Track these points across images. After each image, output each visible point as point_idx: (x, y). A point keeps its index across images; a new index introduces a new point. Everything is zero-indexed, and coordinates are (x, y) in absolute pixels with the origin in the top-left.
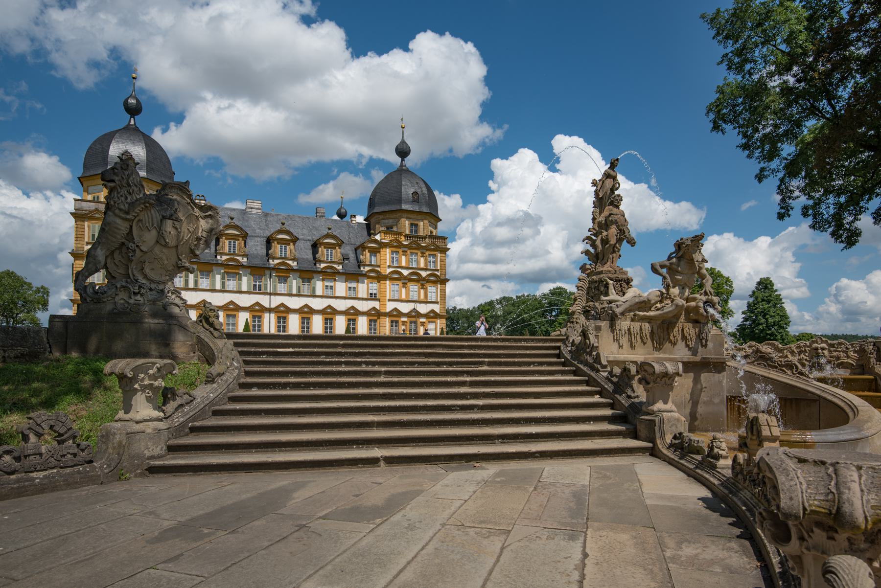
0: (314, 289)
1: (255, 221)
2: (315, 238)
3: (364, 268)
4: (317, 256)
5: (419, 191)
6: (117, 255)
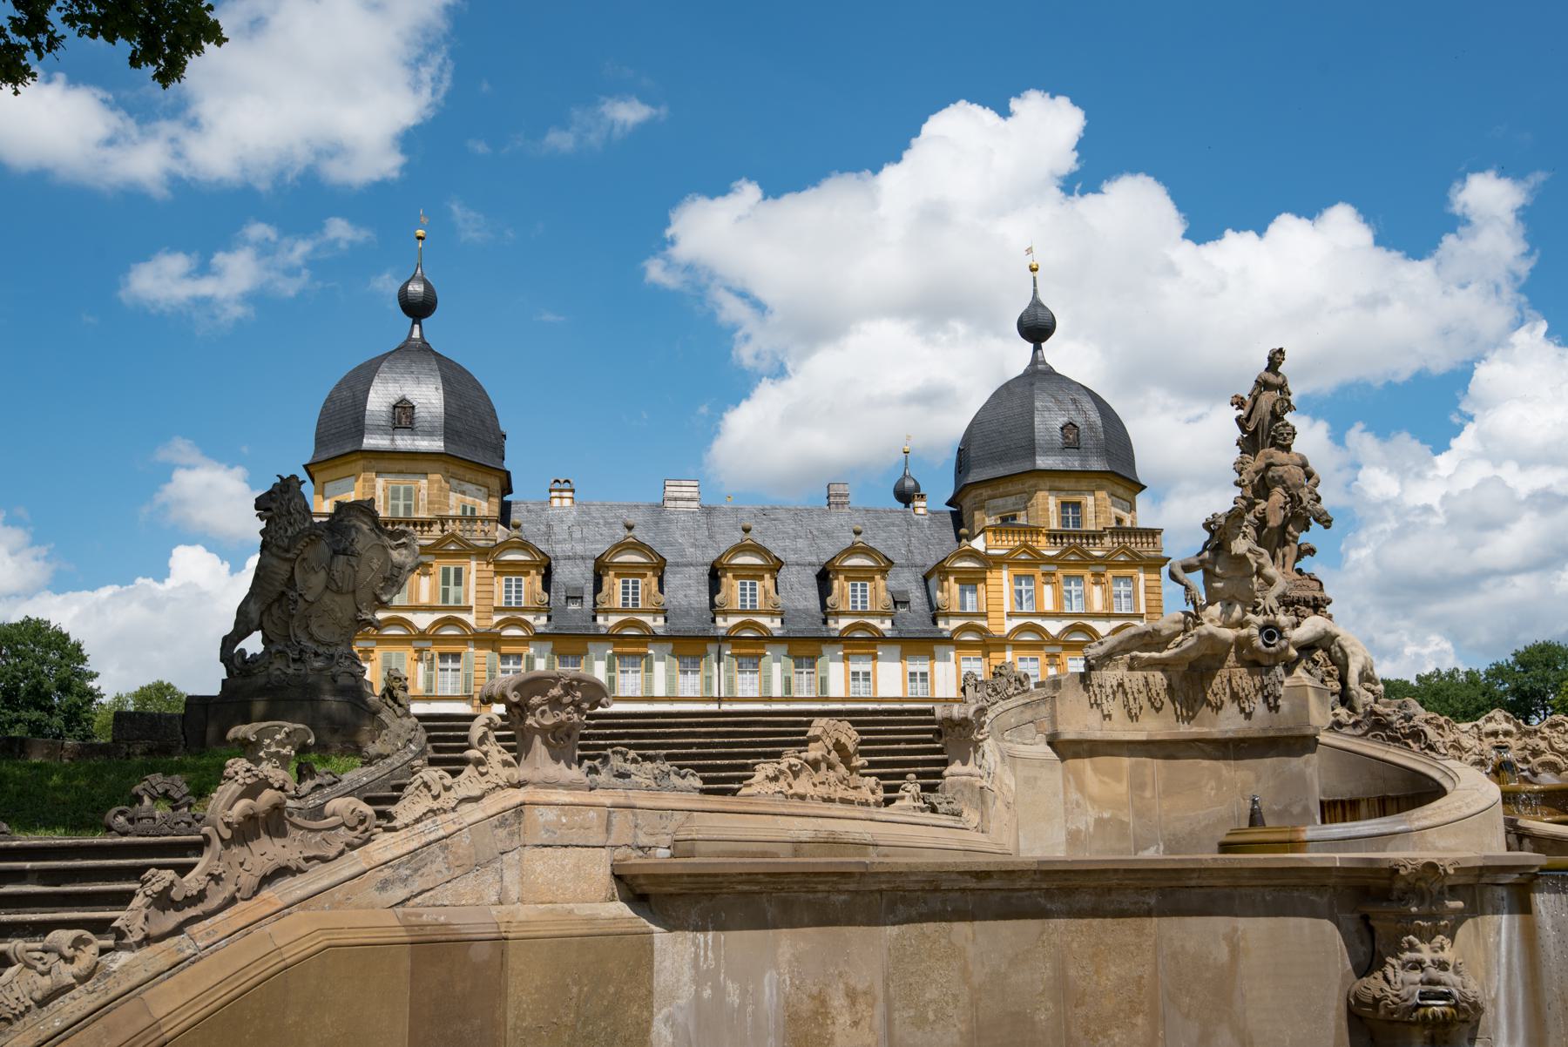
0: (824, 682)
1: (683, 529)
2: (825, 558)
3: (947, 623)
4: (829, 601)
5: (1079, 421)
6: (275, 610)
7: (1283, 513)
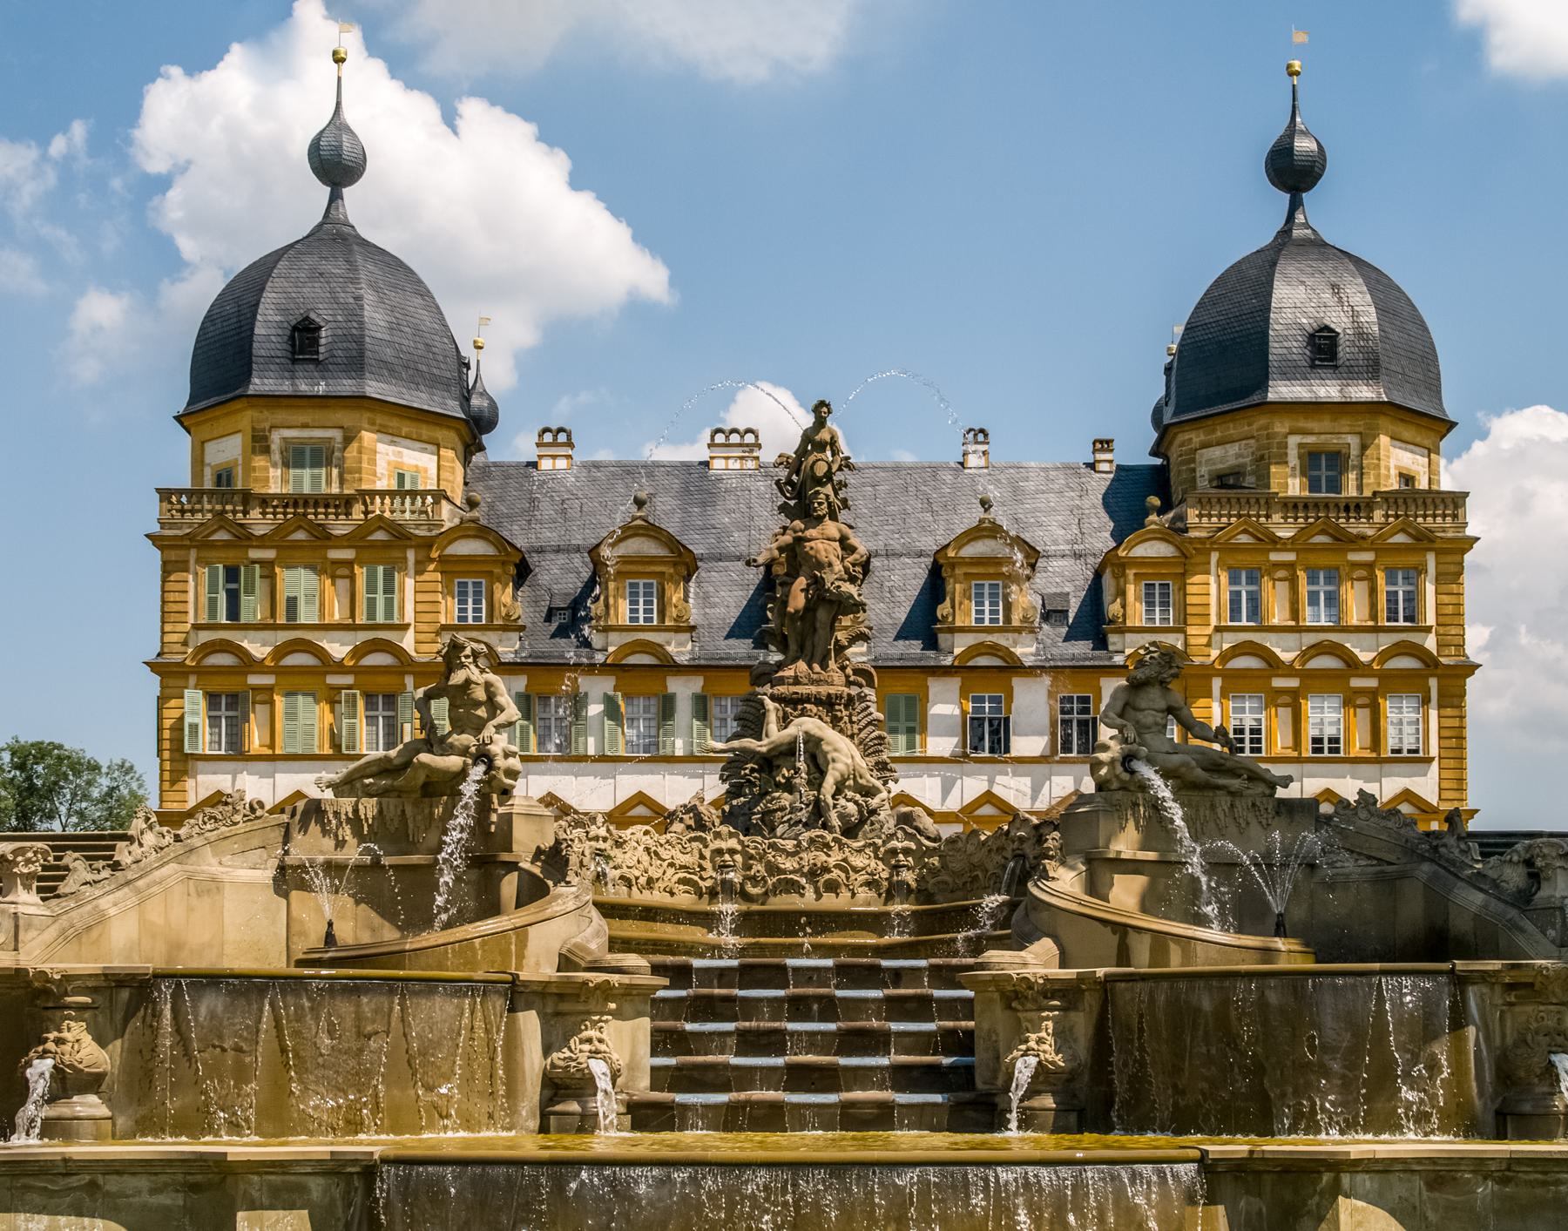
4: (943, 609)
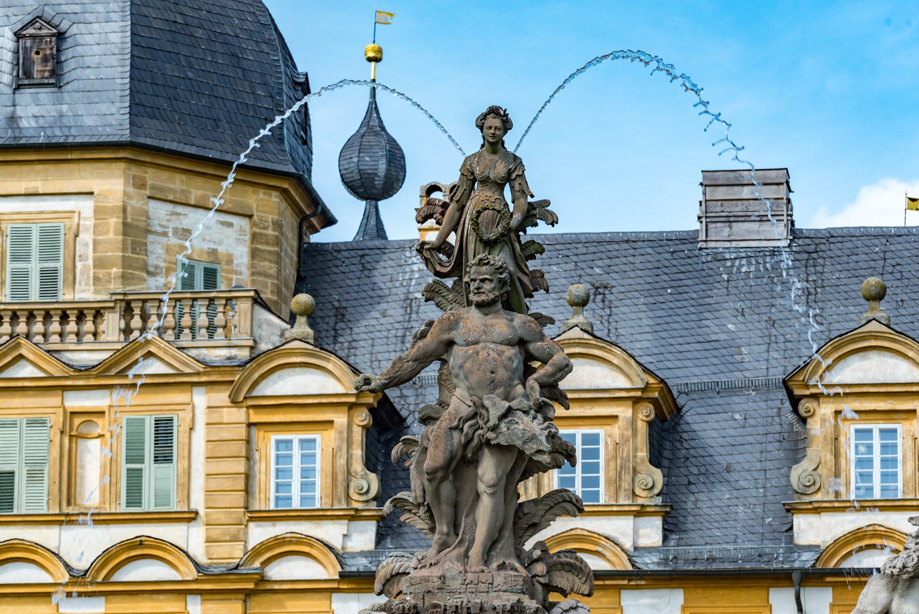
7: (458, 438)
